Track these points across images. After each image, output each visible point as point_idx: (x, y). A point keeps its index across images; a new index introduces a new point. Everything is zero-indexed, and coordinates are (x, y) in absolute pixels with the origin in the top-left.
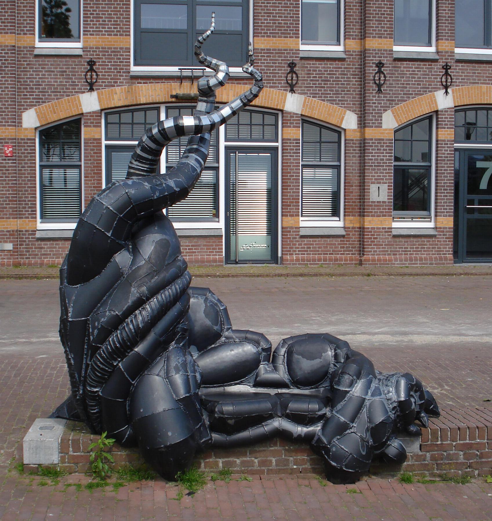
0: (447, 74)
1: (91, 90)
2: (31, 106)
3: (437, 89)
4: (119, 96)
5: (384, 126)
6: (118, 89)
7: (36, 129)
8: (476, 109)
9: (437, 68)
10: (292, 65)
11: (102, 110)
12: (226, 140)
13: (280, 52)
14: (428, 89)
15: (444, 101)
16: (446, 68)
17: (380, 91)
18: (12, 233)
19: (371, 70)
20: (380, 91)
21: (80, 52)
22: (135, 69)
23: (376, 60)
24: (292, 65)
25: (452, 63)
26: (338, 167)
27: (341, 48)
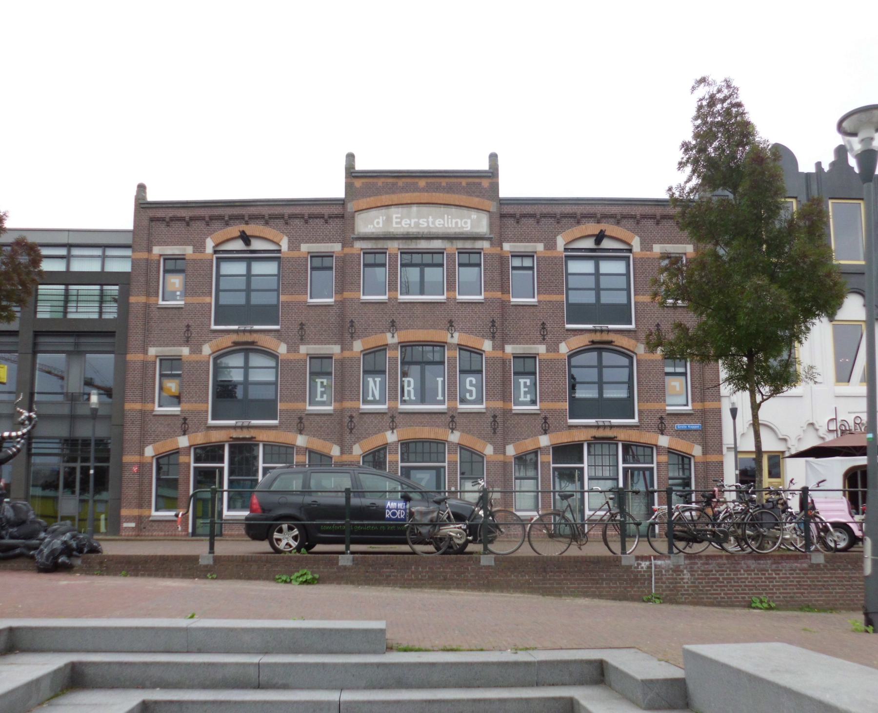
0: (393, 421)
1: (184, 434)
2: (150, 444)
3: (386, 430)
4: (200, 438)
5: (354, 453)
6: (200, 434)
7: (153, 457)
8: (416, 442)
9: (387, 418)
10: (301, 418)
11: (190, 446)
12: (264, 462)
13: (294, 411)
14: (381, 430)
15: (391, 437)
16: (393, 417)
17: (351, 432)
18: (135, 517)
19: (347, 420)
20: (351, 432)
21: (178, 413)
22: (211, 422)
23: (349, 414)
24: (301, 418)
25: (397, 415)
26: (537, 479)
27: (537, 407)
